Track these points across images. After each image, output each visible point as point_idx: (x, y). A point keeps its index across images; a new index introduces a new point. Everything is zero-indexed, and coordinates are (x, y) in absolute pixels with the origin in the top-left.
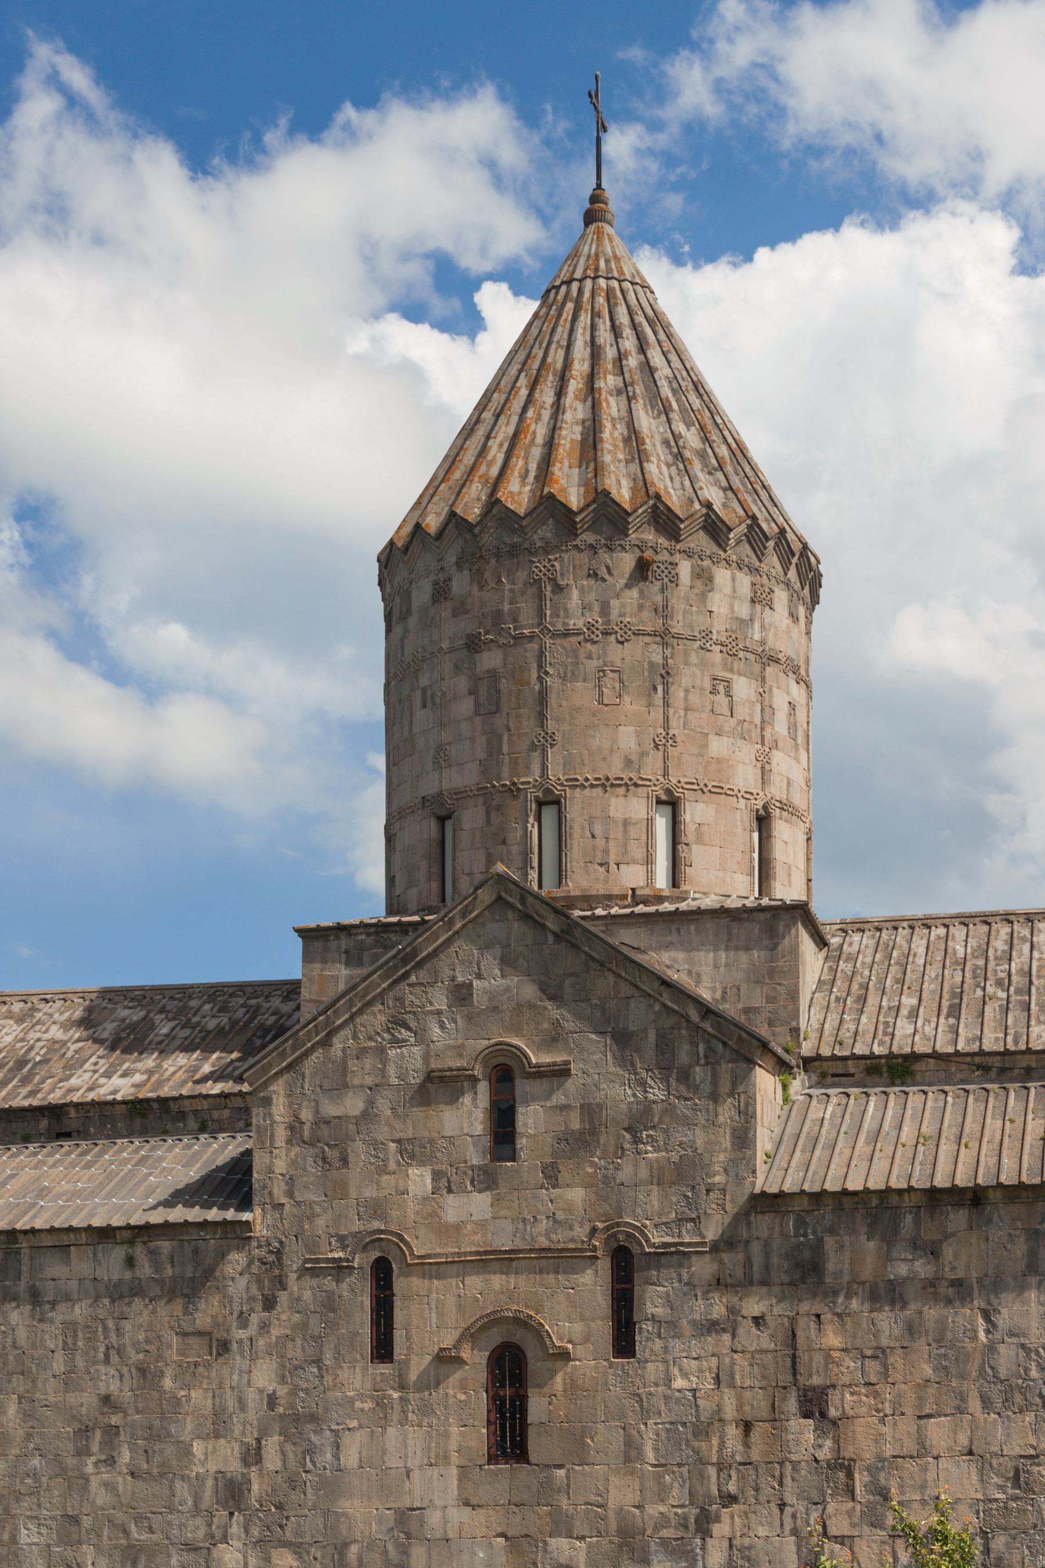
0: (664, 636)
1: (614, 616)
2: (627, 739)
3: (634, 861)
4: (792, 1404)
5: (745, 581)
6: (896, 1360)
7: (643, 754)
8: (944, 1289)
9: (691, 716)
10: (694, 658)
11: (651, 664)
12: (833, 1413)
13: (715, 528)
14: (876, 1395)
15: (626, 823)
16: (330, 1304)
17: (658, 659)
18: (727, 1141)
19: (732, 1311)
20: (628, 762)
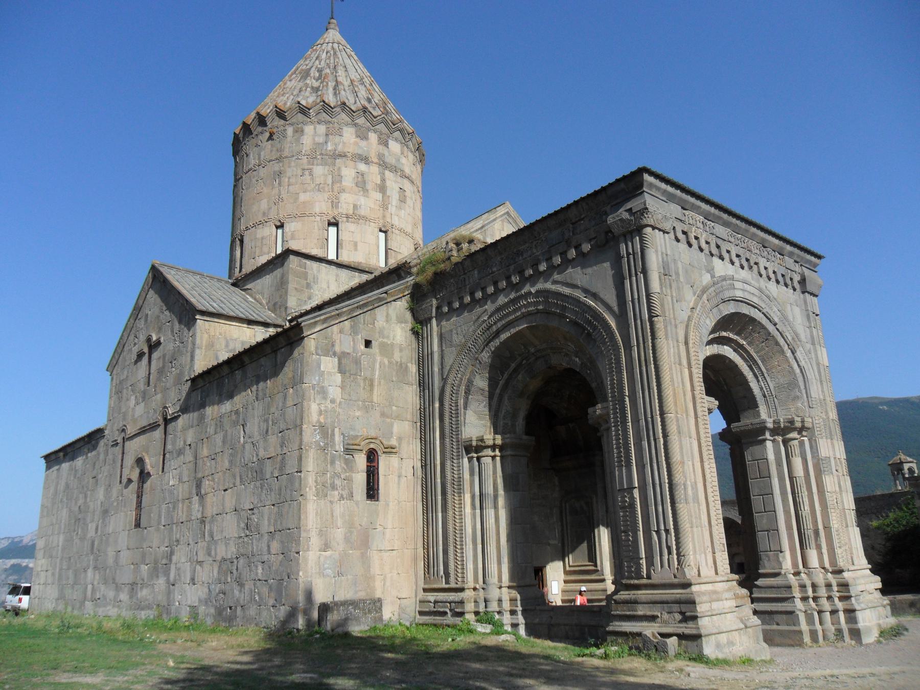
0: (279, 159)
1: (262, 158)
2: (264, 205)
3: (265, 254)
4: (194, 491)
5: (322, 129)
6: (219, 459)
7: (270, 208)
8: (234, 417)
9: (291, 188)
10: (293, 164)
11: (274, 172)
12: (203, 492)
13: (304, 110)
14: (213, 480)
15: (262, 238)
16: (114, 461)
17: (277, 169)
18: (189, 359)
19: (185, 442)
20: (264, 214)
